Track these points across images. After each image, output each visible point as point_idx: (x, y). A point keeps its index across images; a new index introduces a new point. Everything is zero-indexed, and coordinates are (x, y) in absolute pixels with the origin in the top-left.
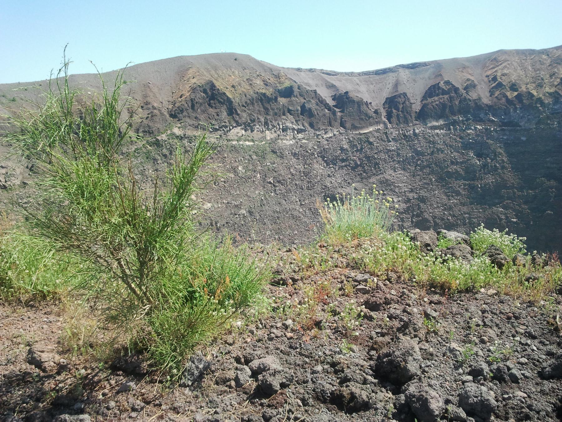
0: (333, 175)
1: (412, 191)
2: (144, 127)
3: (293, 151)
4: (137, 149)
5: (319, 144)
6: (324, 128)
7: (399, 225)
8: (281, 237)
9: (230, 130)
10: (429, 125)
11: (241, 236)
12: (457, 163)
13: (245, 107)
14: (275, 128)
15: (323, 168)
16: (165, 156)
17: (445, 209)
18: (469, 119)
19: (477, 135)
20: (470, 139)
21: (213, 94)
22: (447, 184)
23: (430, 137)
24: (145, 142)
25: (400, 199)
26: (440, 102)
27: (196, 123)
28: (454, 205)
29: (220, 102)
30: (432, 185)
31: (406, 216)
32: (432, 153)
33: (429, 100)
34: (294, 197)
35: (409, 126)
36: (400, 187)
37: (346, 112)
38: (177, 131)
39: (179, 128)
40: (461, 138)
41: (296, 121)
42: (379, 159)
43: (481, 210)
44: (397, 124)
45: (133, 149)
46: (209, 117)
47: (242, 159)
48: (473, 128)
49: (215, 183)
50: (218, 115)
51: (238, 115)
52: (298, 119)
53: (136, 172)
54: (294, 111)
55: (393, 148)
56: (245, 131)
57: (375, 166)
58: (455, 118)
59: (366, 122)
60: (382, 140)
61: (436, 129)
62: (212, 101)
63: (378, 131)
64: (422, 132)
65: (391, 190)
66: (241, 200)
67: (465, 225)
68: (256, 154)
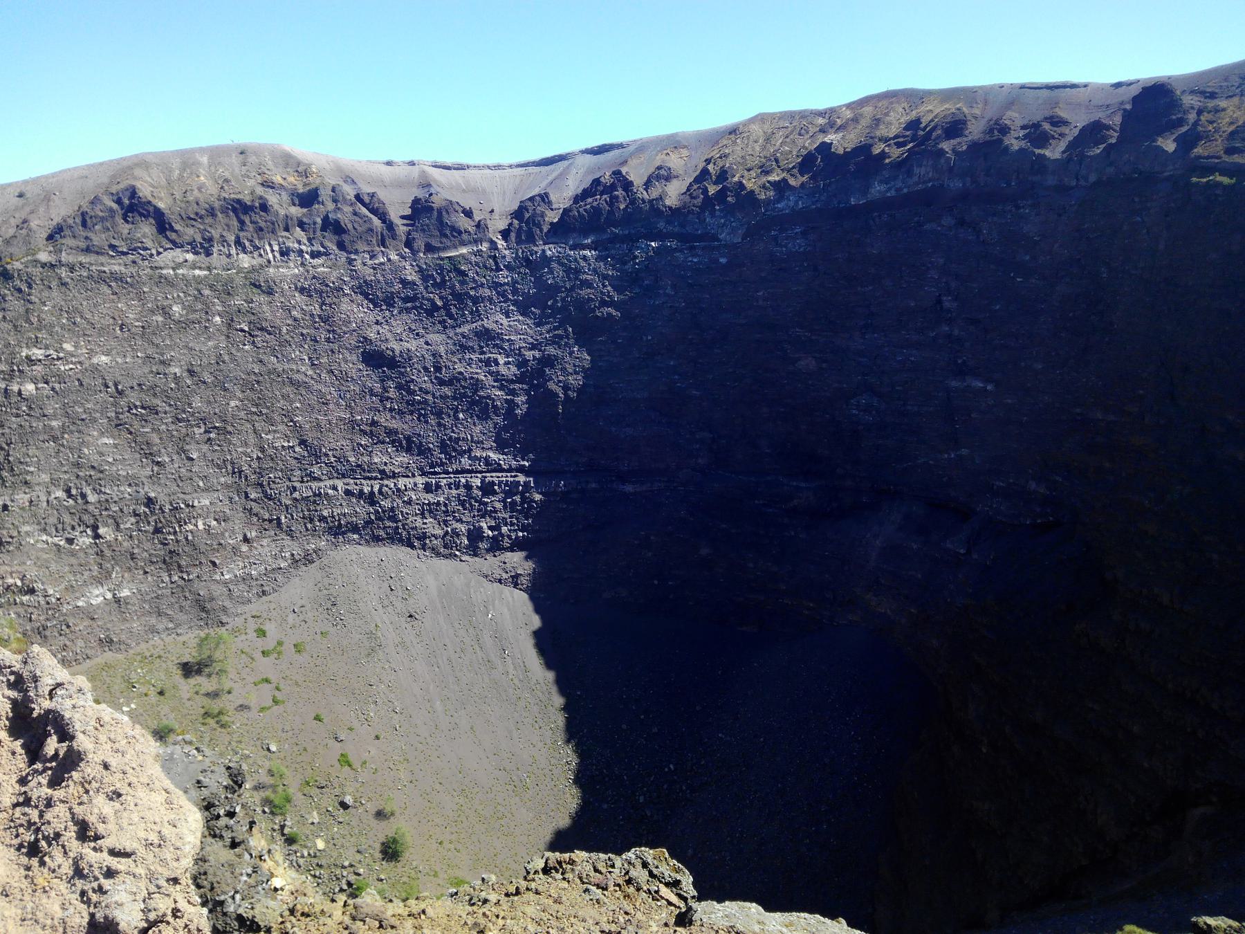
0: (387, 321)
5: (354, 274)
8: (264, 411)
11: (170, 405)
15: (366, 310)
16: (20, 291)
25: (510, 359)
26: (592, 207)
27: (83, 245)
29: (141, 215)
32: (572, 289)
34: (298, 353)
36: (512, 341)
41: (310, 240)
47: (181, 295)
49: (121, 329)
51: (176, 231)
56: (196, 253)
59: (453, 239)
64: (557, 254)
66: (173, 354)
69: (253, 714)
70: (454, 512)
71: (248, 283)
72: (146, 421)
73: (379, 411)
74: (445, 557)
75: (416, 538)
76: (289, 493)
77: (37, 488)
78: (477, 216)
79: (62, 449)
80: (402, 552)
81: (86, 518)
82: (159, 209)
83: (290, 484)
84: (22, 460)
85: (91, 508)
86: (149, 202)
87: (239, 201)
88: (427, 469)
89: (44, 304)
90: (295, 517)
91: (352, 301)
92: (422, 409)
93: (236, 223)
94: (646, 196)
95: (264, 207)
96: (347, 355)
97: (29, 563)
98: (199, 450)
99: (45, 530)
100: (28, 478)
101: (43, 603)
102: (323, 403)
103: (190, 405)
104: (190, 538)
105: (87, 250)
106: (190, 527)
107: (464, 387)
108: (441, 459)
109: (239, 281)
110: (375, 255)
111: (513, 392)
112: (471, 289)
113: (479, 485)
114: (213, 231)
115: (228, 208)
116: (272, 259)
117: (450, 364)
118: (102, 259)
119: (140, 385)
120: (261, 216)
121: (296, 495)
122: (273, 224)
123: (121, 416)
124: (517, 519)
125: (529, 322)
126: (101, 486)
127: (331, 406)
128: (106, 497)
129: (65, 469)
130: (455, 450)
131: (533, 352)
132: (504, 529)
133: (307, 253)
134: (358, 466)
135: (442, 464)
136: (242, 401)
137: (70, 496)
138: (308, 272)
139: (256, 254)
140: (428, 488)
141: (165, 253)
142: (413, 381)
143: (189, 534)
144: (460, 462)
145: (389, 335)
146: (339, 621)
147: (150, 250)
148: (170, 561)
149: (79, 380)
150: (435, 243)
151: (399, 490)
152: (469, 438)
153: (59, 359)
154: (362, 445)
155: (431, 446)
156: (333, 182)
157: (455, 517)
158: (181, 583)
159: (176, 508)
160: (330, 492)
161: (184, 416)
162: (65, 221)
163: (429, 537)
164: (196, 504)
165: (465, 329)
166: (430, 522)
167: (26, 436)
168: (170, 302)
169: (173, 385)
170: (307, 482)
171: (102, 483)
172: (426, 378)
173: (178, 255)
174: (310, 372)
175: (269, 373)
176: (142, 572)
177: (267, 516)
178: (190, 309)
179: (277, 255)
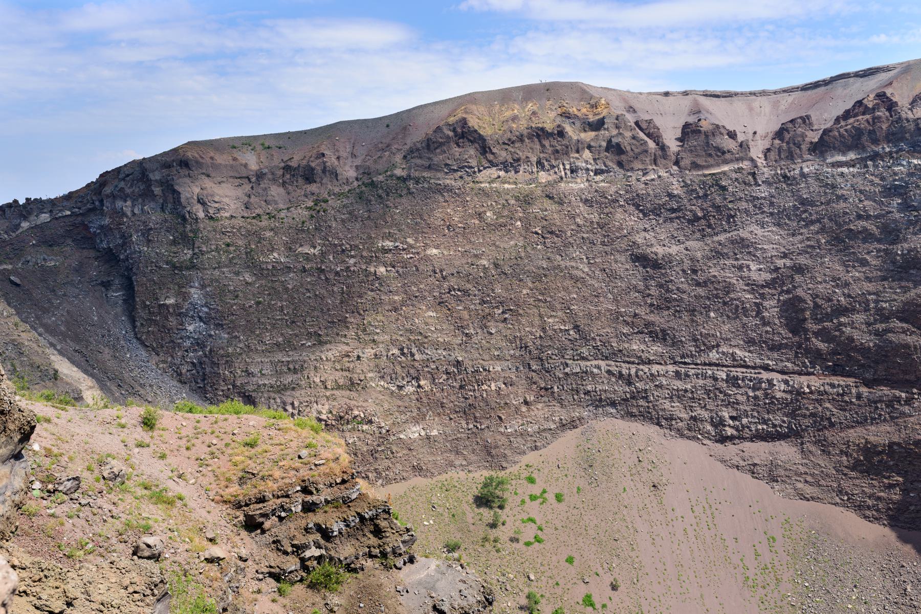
1: (785, 256)
3: (584, 197)
4: (350, 190)
5: (629, 189)
6: (640, 167)
7: (754, 303)
8: (548, 299)
10: (829, 160)
11: (479, 290)
12: (868, 217)
13: (509, 145)
14: (556, 169)
15: (636, 219)
16: (380, 197)
17: (837, 285)
18: (901, 150)
19: (911, 175)
20: (895, 180)
21: (463, 131)
22: (847, 248)
23: (827, 178)
24: (360, 183)
25: (761, 266)
27: (426, 163)
28: (854, 280)
30: (820, 249)
31: (770, 291)
32: (828, 203)
33: (843, 123)
34: (578, 253)
35: (795, 163)
37: (686, 146)
40: (883, 179)
41: (595, 160)
42: (735, 209)
43: (898, 290)
44: (776, 161)
45: (347, 190)
47: (494, 203)
48: (905, 163)
49: (449, 229)
51: (493, 154)
52: (597, 157)
54: (595, 147)
55: (763, 195)
56: (507, 172)
57: (729, 220)
58: (876, 149)
59: (716, 158)
60: (745, 184)
61: (841, 166)
62: (461, 140)
63: (740, 170)
64: (814, 171)
65: (749, 253)
67: (869, 310)
68: (517, 199)
69: (520, 546)
70: (699, 400)
71: (544, 195)
72: (460, 300)
73: (641, 305)
74: (688, 438)
75: (664, 418)
76: (562, 368)
77: (381, 346)
78: (741, 137)
79: (400, 318)
80: (651, 430)
81: (412, 371)
82: (482, 136)
83: (563, 361)
85: (416, 364)
86: (476, 131)
87: (542, 129)
88: (678, 359)
89: (396, 207)
90: (565, 388)
91: (625, 211)
92: (678, 306)
93: (538, 147)
94: (910, 116)
95: (561, 133)
96: (618, 256)
97: (370, 401)
98: (496, 327)
99: (383, 377)
100: (376, 337)
101: (377, 432)
102: (596, 296)
103: (493, 290)
104: (485, 396)
105: (429, 168)
106: (485, 387)
107: (716, 289)
108: (691, 352)
109: (538, 192)
110: (647, 173)
111: (763, 296)
112: (730, 202)
113: (725, 378)
114: (521, 154)
115: (534, 135)
116: (564, 176)
117: (705, 268)
118: (439, 175)
119: (458, 273)
120: (558, 141)
121: (567, 370)
122: (567, 147)
123: (443, 296)
124: (758, 412)
125: (782, 233)
126: (424, 347)
127: (601, 299)
128: (428, 357)
129: (401, 333)
130: (705, 345)
131: (784, 260)
132: (745, 421)
133: (592, 171)
134: (620, 351)
135: (692, 356)
136: (532, 290)
137: (403, 354)
138: (591, 186)
139: (552, 172)
140: (678, 375)
141: (484, 171)
142: (671, 281)
143: (484, 393)
144: (708, 355)
145: (654, 241)
146: (594, 481)
147: (473, 168)
148: (467, 412)
149: (416, 266)
150: (700, 161)
151: (652, 375)
152: (718, 334)
153: (404, 249)
154: (624, 334)
155: (683, 339)
156: (619, 113)
157: (700, 404)
158: (475, 430)
159: (477, 371)
160: (595, 371)
162: (415, 145)
163: (675, 419)
164: (491, 369)
165: (722, 238)
166: (678, 407)
167: (376, 305)
168: (484, 209)
169: (482, 274)
170: (577, 360)
171: (426, 346)
172: (683, 280)
173: (493, 172)
174: (586, 270)
175: (555, 268)
176: (448, 418)
177: (542, 386)
178: (499, 215)
179: (568, 173)
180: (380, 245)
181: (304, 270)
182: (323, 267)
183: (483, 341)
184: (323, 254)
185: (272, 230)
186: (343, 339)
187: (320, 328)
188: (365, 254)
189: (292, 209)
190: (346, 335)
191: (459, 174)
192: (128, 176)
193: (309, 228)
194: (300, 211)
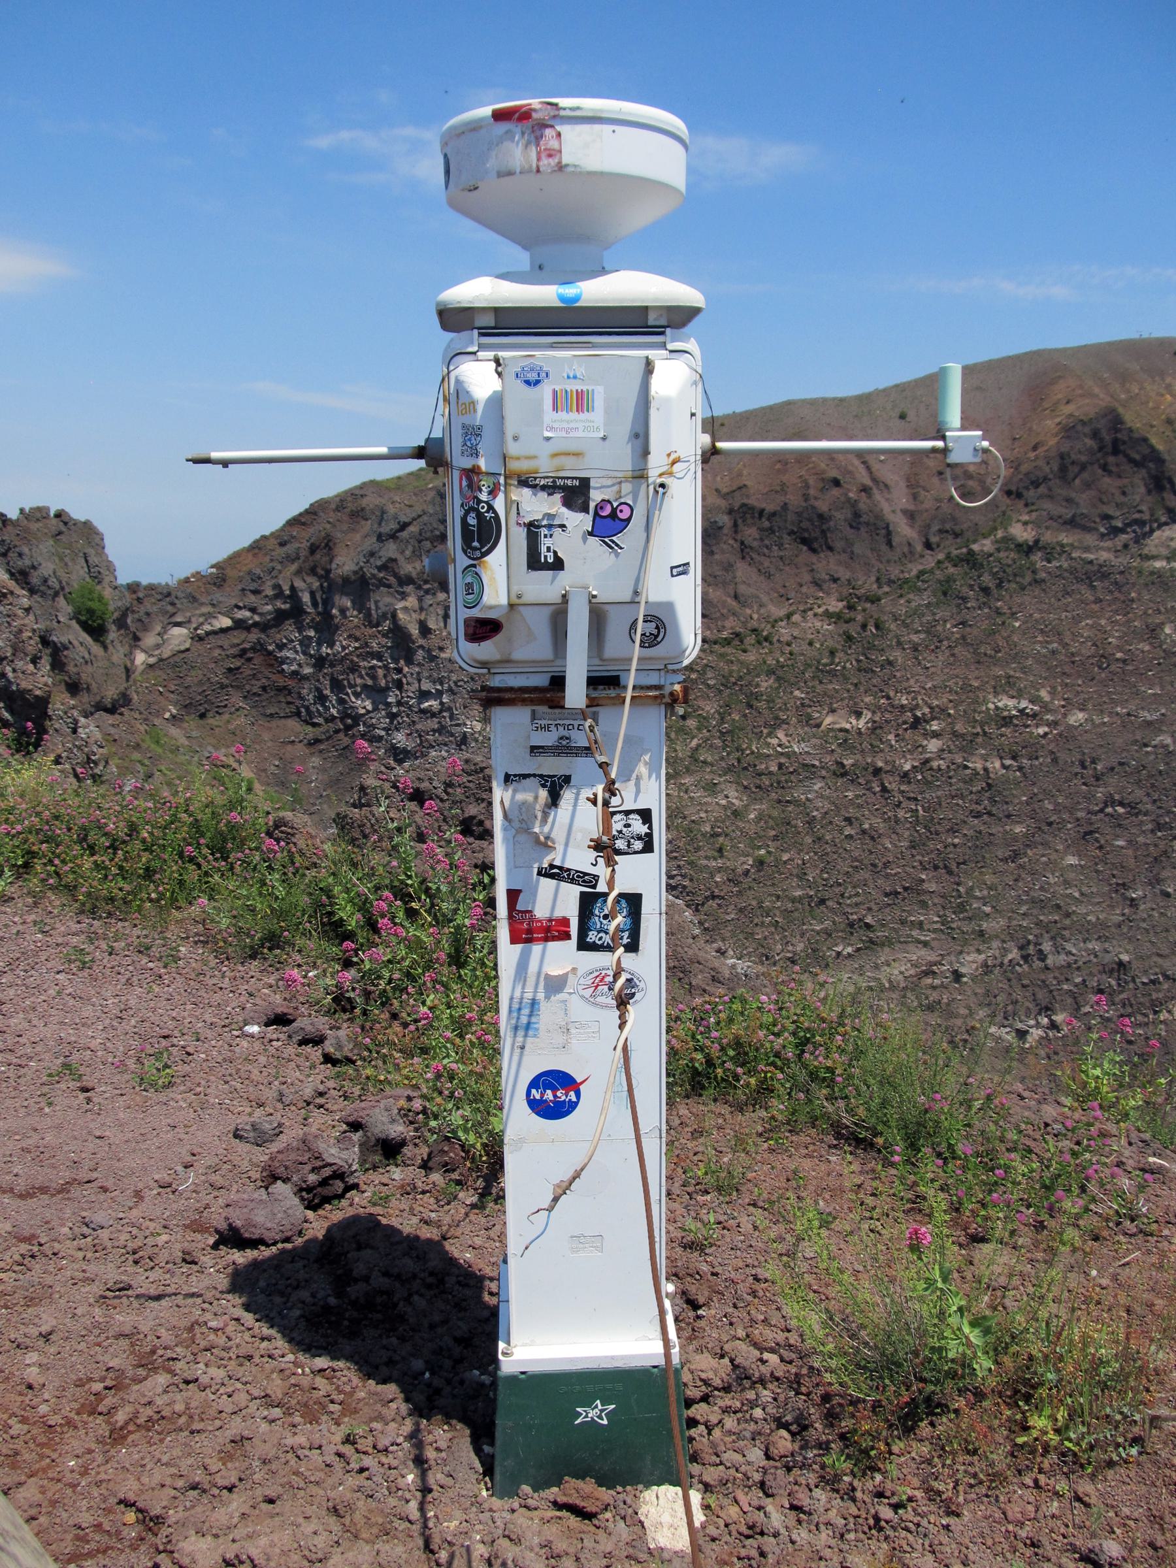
2: (943, 521)
4: (922, 573)
9: (1152, 531)
16: (986, 590)
21: (1115, 442)
27: (1068, 513)
29: (1131, 461)
38: (1022, 533)
39: (1025, 523)
45: (914, 572)
46: (1101, 500)
50: (1124, 493)
53: (917, 626)
62: (1111, 459)
84: (978, 894)
86: (1145, 440)
105: (1072, 523)
118: (1090, 539)
129: (1024, 909)
161: (1167, 820)
171: (1066, 933)
180: (991, 706)
181: (841, 772)
182: (880, 764)
183: (1156, 914)
184: (875, 728)
185: (771, 672)
186: (915, 933)
187: (870, 909)
188: (959, 727)
189: (796, 618)
190: (921, 923)
191: (1124, 537)
192: (404, 526)
193: (844, 668)
194: (818, 624)
